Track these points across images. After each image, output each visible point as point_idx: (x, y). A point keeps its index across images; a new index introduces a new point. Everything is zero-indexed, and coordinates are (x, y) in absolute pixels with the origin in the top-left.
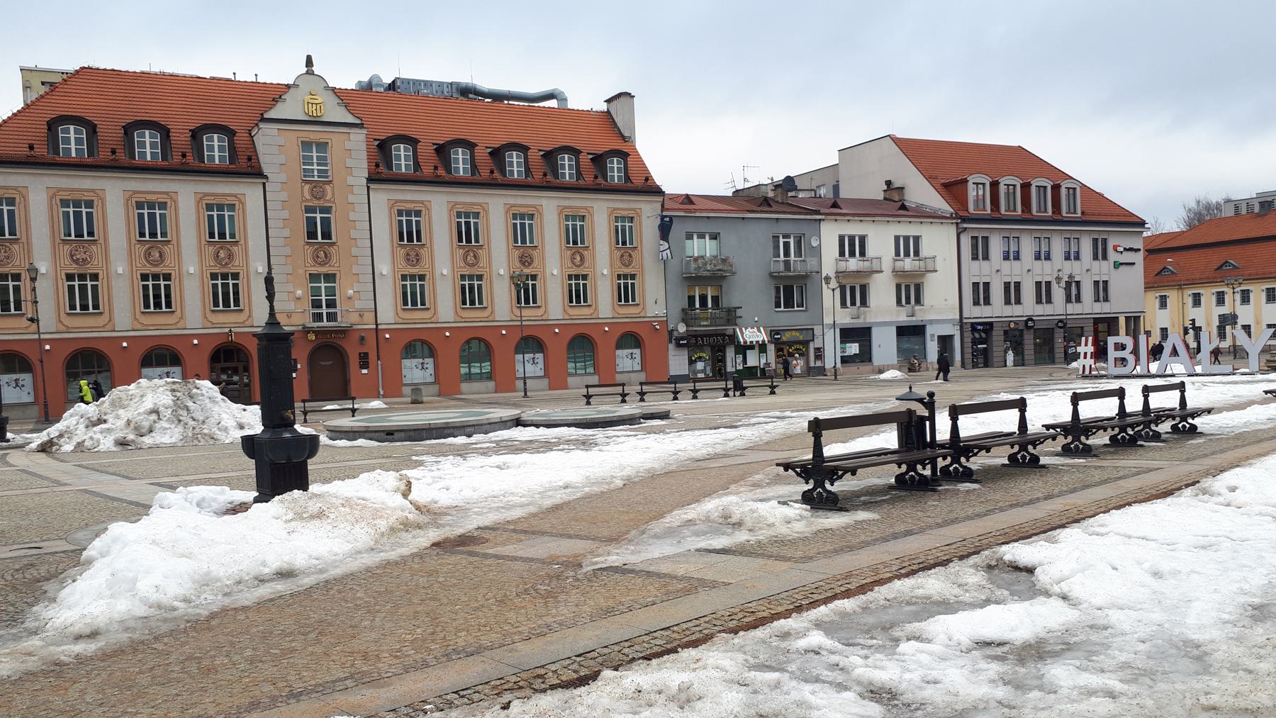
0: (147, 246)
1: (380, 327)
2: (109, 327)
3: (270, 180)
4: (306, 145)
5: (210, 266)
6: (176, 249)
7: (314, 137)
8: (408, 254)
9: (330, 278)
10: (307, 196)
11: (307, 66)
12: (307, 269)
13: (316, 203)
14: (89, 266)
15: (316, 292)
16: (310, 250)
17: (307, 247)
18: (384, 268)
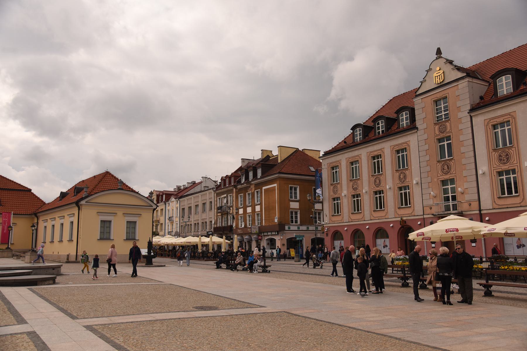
0: (375, 177)
1: (482, 212)
2: (363, 219)
3: (419, 129)
4: (436, 102)
5: (397, 184)
6: (385, 177)
7: (439, 96)
8: (500, 156)
9: (452, 181)
10: (437, 132)
11: (436, 54)
12: (439, 178)
13: (442, 136)
14: (357, 190)
15: (446, 191)
16: (439, 165)
17: (438, 164)
18: (483, 168)
